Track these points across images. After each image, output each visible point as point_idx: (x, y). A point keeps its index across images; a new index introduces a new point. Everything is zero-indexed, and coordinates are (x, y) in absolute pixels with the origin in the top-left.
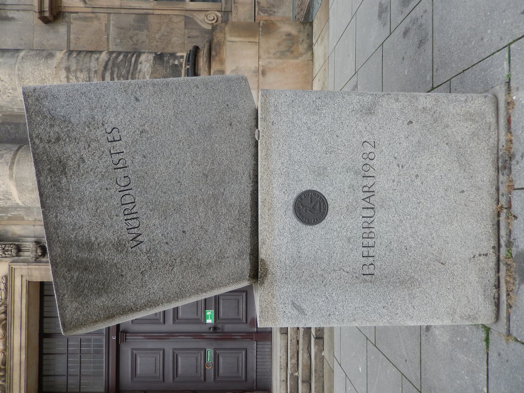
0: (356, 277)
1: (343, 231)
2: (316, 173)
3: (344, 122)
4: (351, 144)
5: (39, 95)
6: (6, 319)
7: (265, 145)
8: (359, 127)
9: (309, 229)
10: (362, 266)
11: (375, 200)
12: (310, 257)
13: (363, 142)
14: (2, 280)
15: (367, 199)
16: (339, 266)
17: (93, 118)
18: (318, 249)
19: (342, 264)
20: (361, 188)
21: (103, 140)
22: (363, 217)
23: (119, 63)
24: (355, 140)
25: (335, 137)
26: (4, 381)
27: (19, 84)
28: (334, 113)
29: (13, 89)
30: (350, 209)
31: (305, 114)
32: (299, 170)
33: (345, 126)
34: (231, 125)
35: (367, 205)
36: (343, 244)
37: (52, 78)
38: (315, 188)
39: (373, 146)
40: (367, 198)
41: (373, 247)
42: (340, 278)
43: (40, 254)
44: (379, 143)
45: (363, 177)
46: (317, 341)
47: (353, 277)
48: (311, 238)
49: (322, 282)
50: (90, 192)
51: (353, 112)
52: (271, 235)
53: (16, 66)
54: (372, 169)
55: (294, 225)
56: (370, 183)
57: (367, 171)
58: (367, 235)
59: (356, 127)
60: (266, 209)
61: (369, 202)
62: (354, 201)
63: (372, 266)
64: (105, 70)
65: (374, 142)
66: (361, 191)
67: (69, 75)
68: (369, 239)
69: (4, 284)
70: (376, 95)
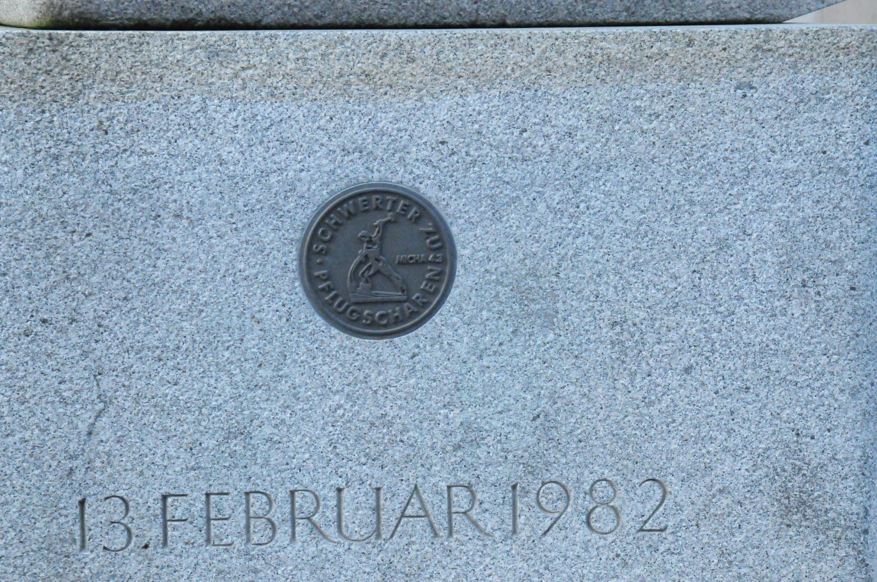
0: (71, 471)
1: (276, 407)
2: (530, 282)
3: (750, 397)
4: (653, 432)
7: (648, 52)
8: (729, 460)
9: (284, 255)
10: (121, 493)
11: (414, 543)
12: (160, 263)
13: (661, 479)
15: (418, 505)
16: (122, 393)
18: (195, 297)
19: (127, 404)
20: (465, 477)
22: (339, 490)
24: (673, 447)
25: (685, 360)
28: (787, 353)
30: (374, 434)
31: (785, 229)
32: (541, 207)
33: (730, 404)
35: (391, 507)
36: (218, 408)
38: (463, 282)
39: (648, 526)
40: (423, 507)
41: (208, 541)
42: (64, 401)
44: (662, 549)
45: (514, 487)
47: (71, 458)
48: (242, 266)
49: (44, 321)
51: (790, 437)
52: (252, 85)
54: (548, 523)
55: (302, 188)
56: (487, 515)
57: (539, 503)
58: (261, 513)
59: (726, 450)
60: (368, 62)
61: (407, 513)
62: (409, 451)
63: (123, 539)
65: (663, 525)
66: (452, 481)
68: (243, 523)
70: (866, 532)
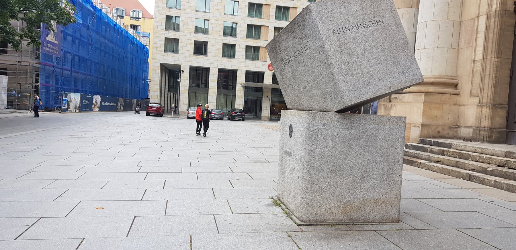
5: (309, 12)
17: (308, 37)
21: (304, 44)
46: (468, 175)
50: (290, 44)
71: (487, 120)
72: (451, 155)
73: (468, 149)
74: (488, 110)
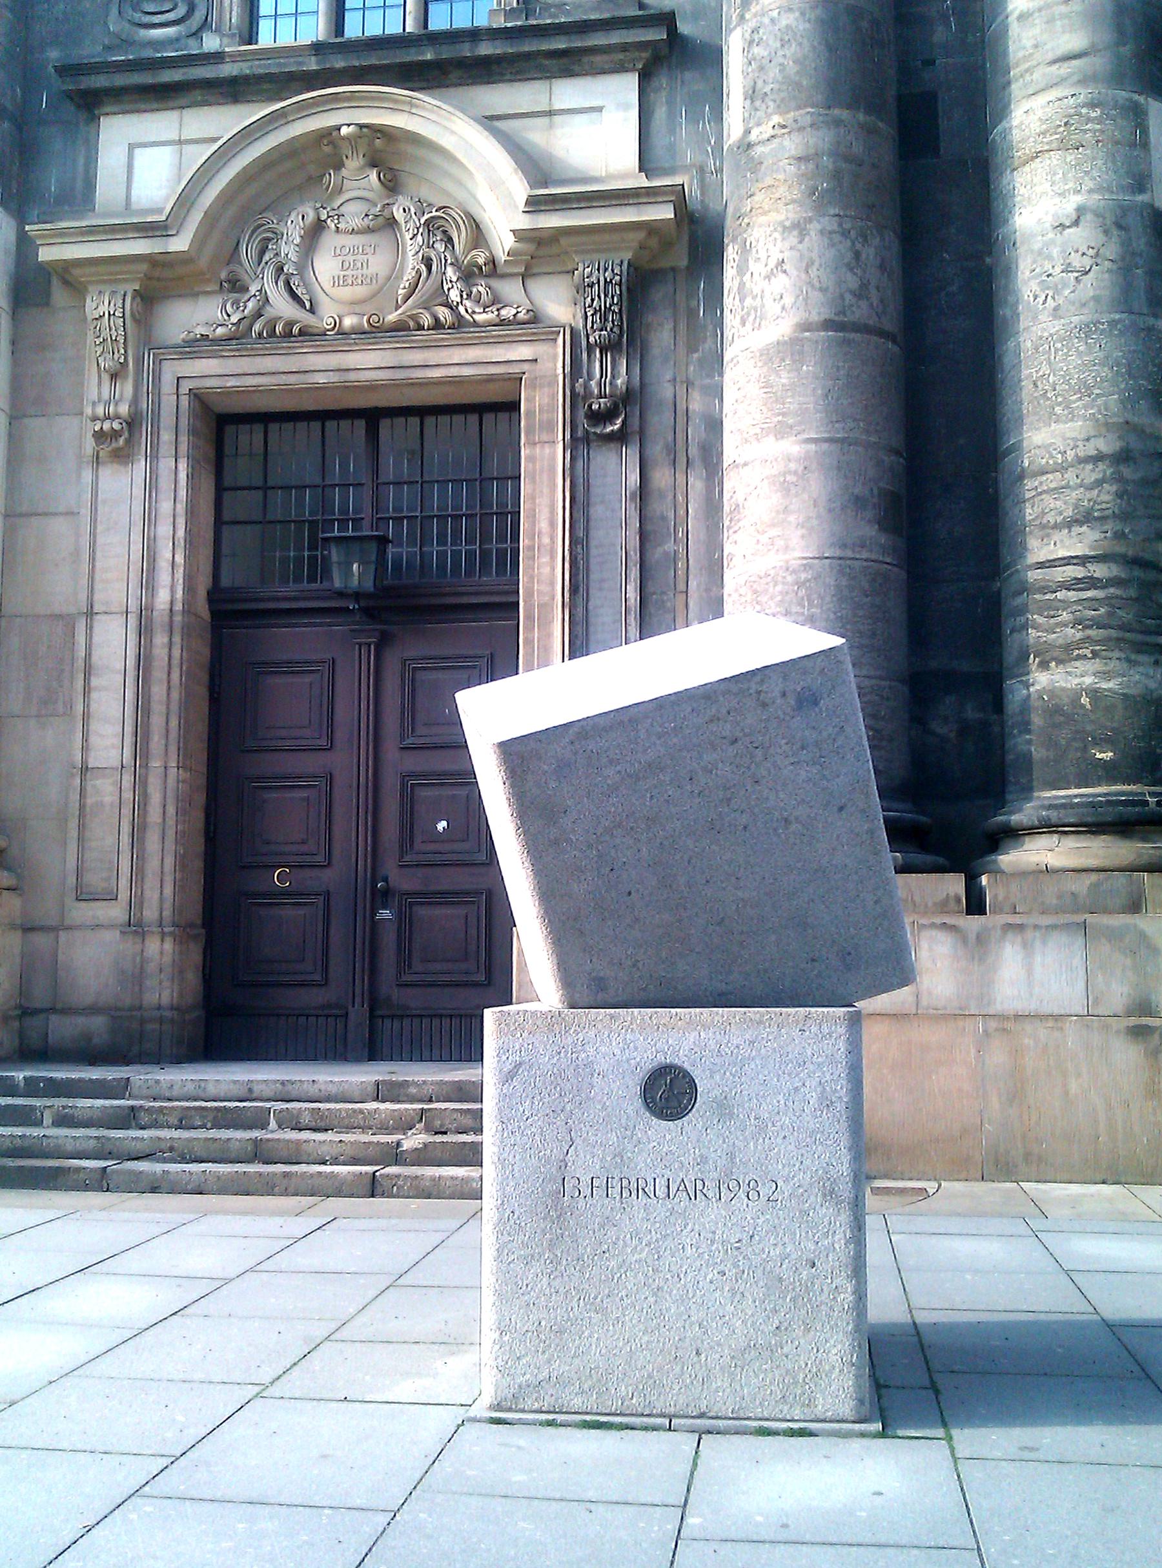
3: (809, 1149)
6: (420, 328)
14: (524, 311)
23: (1152, 601)
26: (260, 334)
27: (1073, 325)
29: (1056, 309)
34: (813, 960)
37: (1094, 414)
43: (595, 407)
46: (369, 1179)
53: (1124, 316)
64: (1128, 562)
67: (1107, 462)
69: (514, 315)
71: (166, 984)
72: (174, 1120)
73: (212, 1090)
74: (168, 946)
